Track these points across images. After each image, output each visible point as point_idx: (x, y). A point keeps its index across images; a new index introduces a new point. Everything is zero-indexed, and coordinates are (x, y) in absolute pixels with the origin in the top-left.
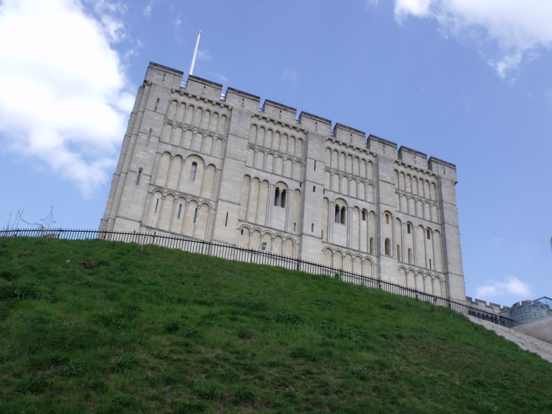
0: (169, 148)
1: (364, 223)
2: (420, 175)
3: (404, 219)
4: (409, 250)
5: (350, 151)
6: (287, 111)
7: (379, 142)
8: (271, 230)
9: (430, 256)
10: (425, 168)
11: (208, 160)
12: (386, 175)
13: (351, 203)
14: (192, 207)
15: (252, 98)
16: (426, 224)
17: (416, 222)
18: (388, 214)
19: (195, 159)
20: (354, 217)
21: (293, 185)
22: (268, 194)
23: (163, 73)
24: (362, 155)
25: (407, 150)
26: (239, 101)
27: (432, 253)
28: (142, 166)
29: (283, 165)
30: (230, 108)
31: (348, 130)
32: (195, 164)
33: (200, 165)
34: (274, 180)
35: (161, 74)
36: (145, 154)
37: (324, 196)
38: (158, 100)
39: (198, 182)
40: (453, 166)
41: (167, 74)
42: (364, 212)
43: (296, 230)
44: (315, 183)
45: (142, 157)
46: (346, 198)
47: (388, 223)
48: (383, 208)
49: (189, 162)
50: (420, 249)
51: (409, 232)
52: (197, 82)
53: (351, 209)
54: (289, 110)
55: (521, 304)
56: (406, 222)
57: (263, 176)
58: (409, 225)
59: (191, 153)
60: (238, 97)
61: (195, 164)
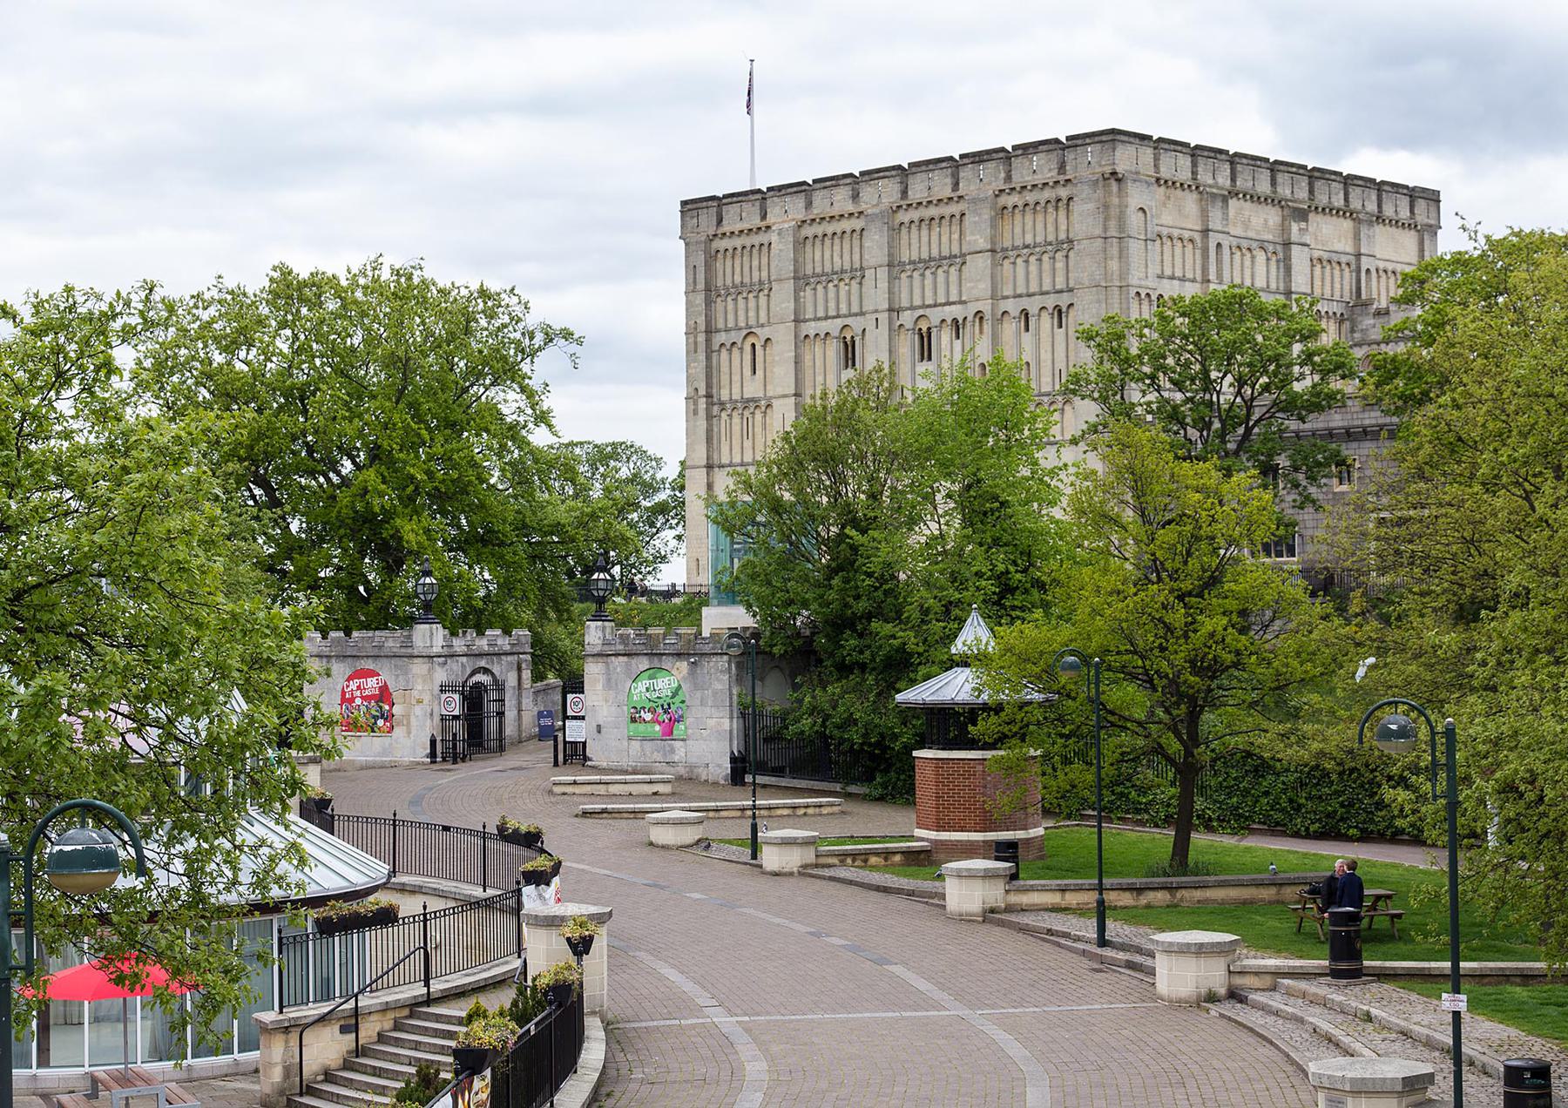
1: (958, 344)
2: (1048, 194)
3: (1012, 306)
5: (933, 211)
11: (763, 333)
15: (795, 189)
16: (1050, 301)
17: (1033, 306)
18: (979, 315)
19: (751, 340)
20: (944, 338)
21: (856, 324)
22: (833, 350)
24: (955, 209)
25: (1020, 152)
27: (1063, 355)
29: (849, 292)
31: (924, 168)
32: (753, 345)
34: (834, 326)
37: (899, 323)
39: (759, 372)
42: (955, 321)
44: (876, 311)
47: (981, 332)
49: (748, 348)
50: (1046, 356)
54: (841, 182)
56: (1017, 314)
57: (824, 326)
58: (1025, 314)
59: (745, 332)
61: (753, 345)
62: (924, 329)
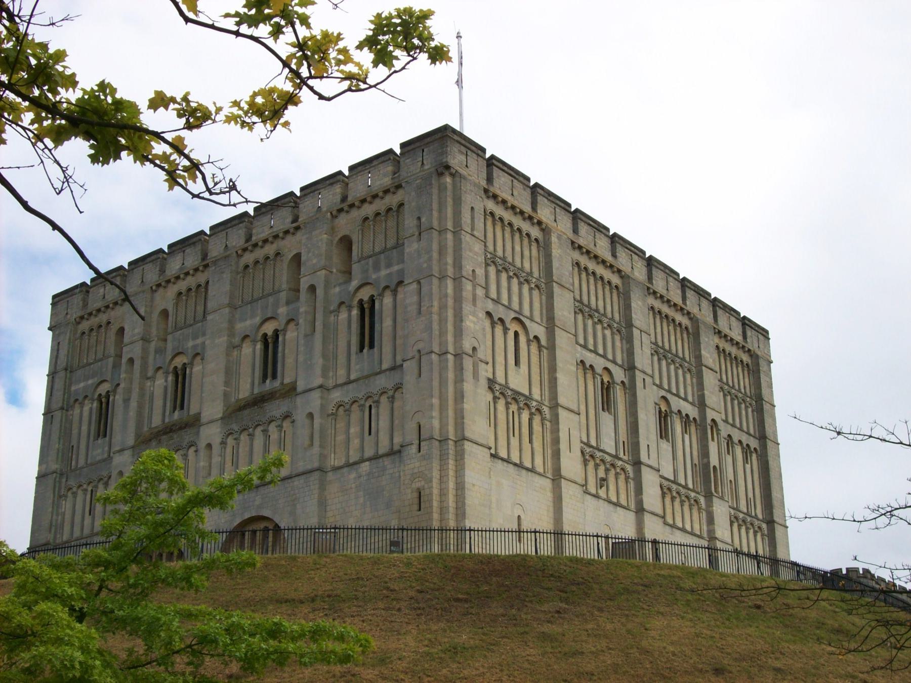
0: (490, 306)
4: (731, 481)
6: (601, 232)
7: (695, 291)
8: (606, 456)
9: (750, 495)
10: (738, 338)
12: (708, 355)
13: (677, 404)
14: (525, 416)
23: (463, 149)
26: (551, 212)
28: (476, 345)
30: (544, 226)
31: (662, 268)
32: (516, 334)
33: (522, 339)
35: (462, 153)
36: (474, 319)
38: (472, 208)
40: (764, 333)
41: (469, 153)
43: (626, 453)
45: (472, 325)
46: (669, 396)
47: (713, 439)
48: (710, 415)
51: (728, 453)
52: (503, 170)
53: (675, 415)
55: (844, 572)
57: (590, 358)
60: (548, 203)
62: (663, 410)
